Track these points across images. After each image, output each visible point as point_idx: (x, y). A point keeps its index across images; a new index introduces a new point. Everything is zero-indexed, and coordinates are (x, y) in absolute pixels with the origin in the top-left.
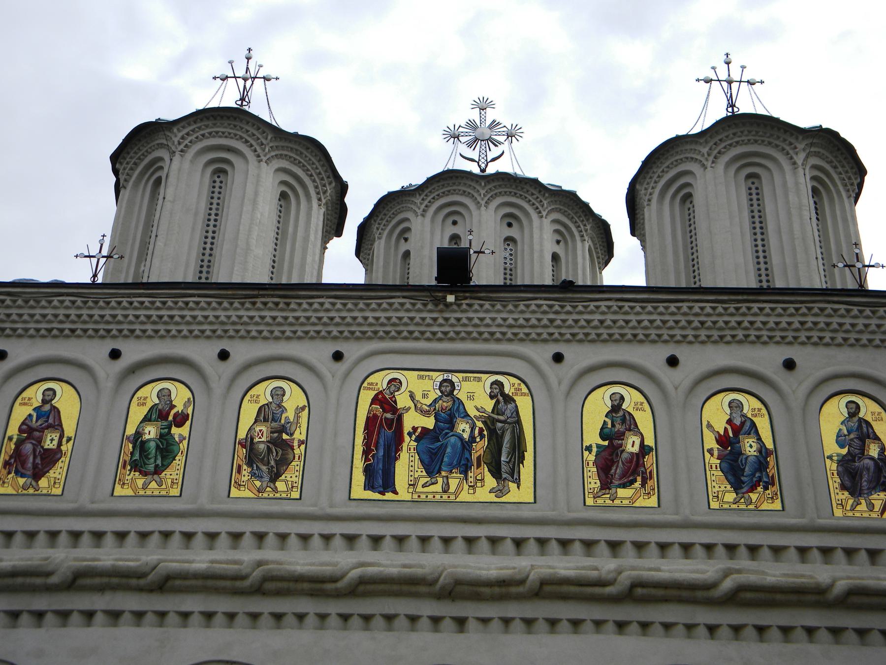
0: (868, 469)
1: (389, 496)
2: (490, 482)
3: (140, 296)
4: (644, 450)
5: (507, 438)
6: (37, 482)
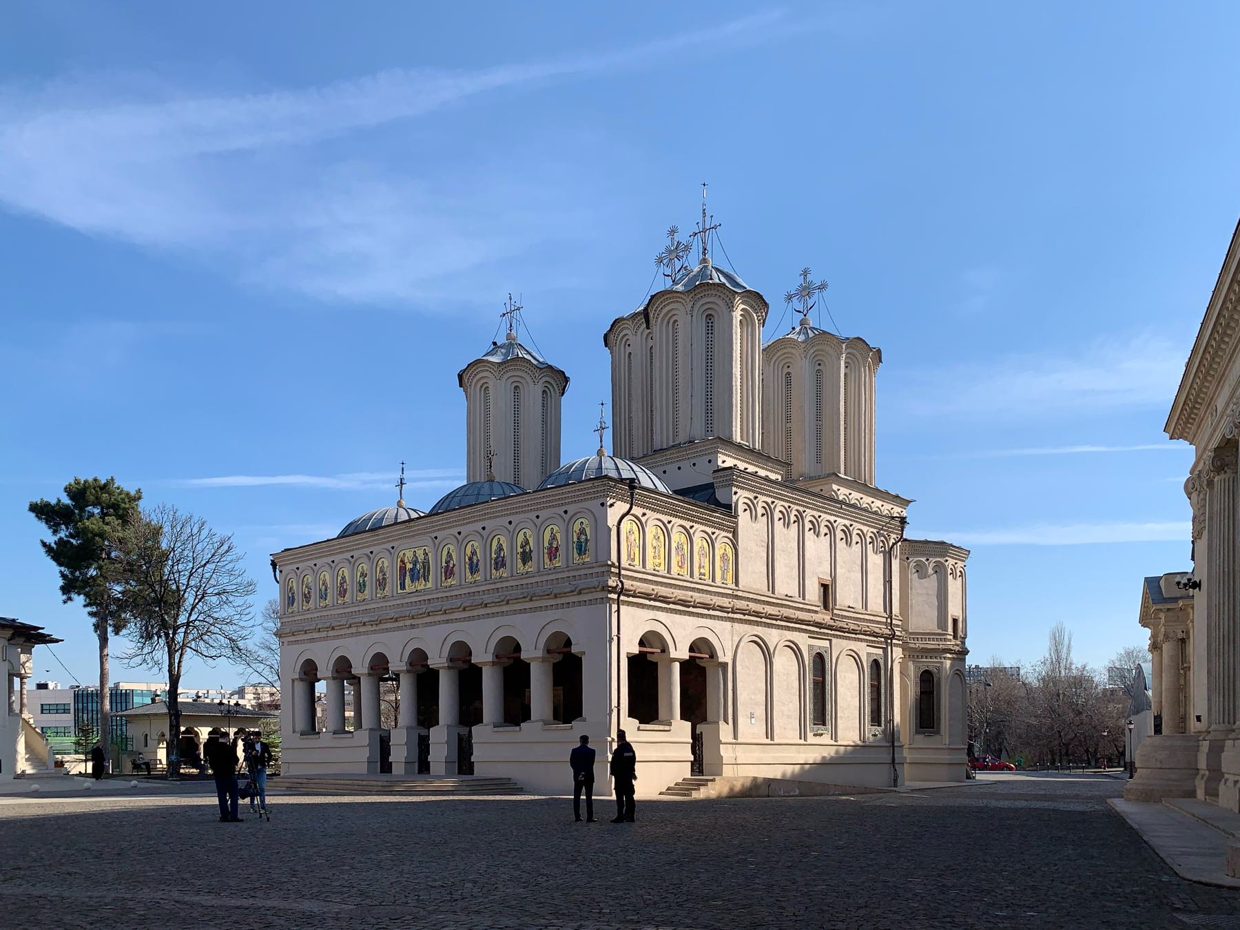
1: (405, 591)
2: (424, 582)
4: (454, 565)
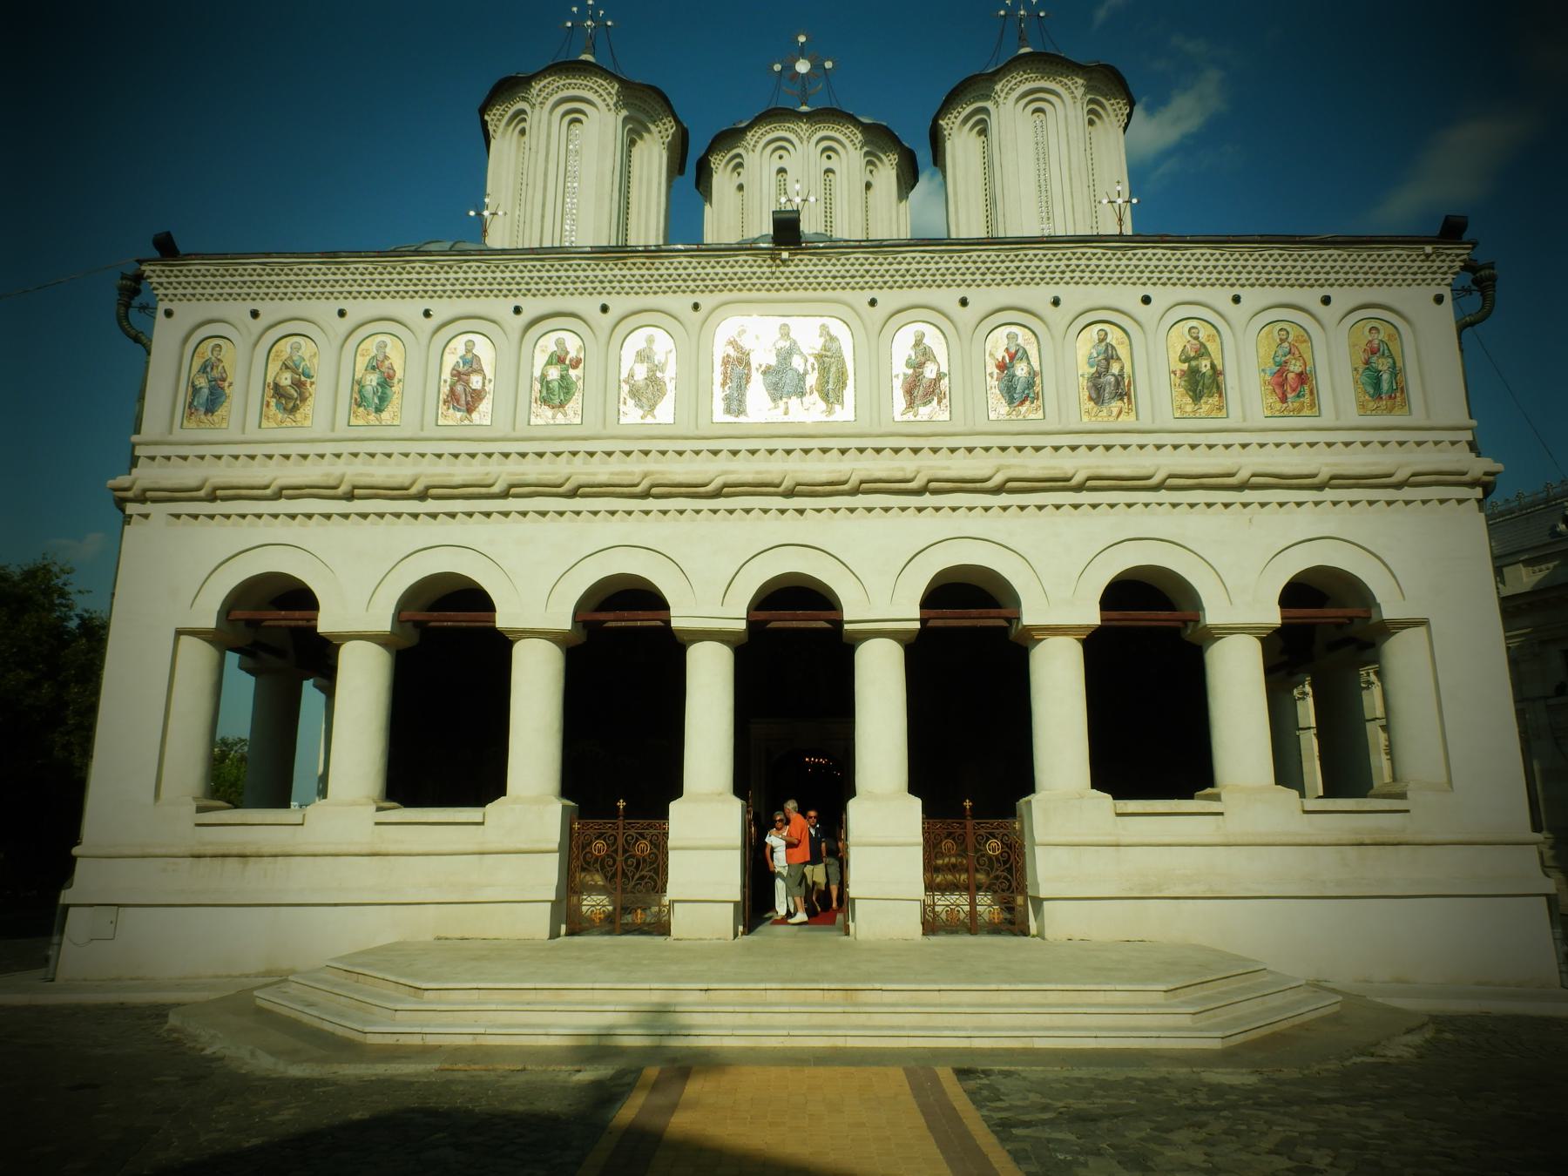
0: (1110, 383)
2: (822, 405)
3: (532, 259)
4: (940, 376)
5: (833, 369)
6: (470, 415)
